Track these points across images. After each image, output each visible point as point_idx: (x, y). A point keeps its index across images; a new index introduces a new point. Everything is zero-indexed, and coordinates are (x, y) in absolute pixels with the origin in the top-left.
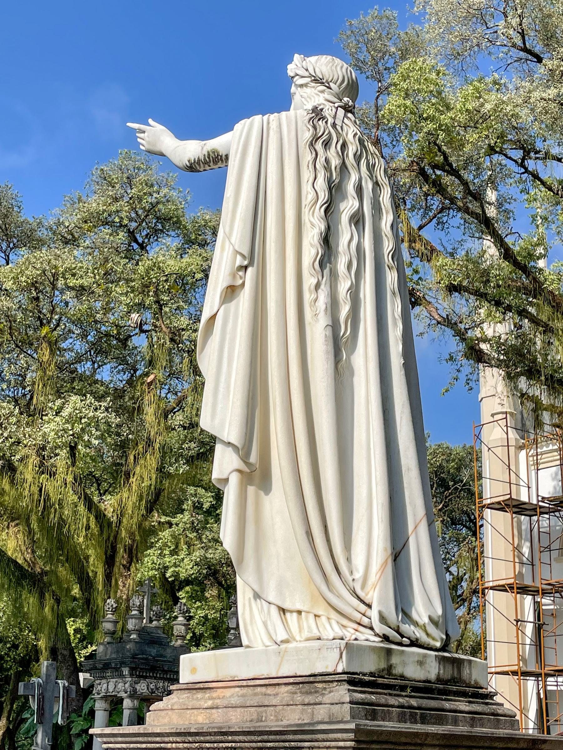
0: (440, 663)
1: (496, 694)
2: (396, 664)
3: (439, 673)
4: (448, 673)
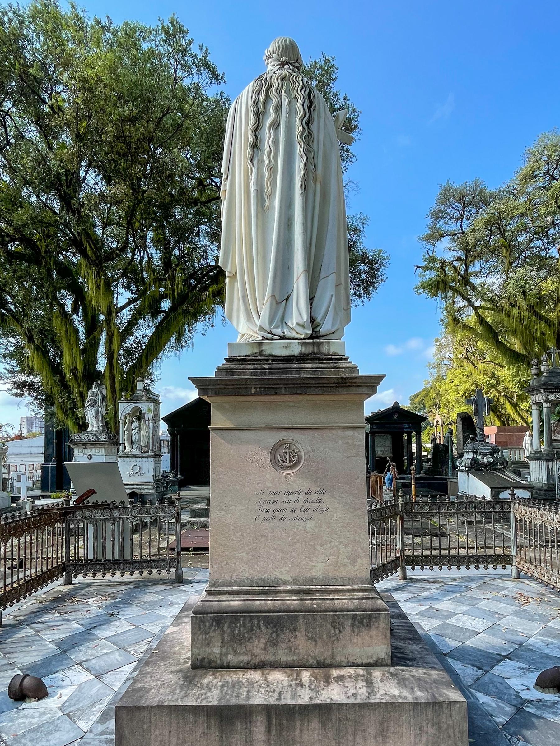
0: (302, 346)
4: (310, 349)
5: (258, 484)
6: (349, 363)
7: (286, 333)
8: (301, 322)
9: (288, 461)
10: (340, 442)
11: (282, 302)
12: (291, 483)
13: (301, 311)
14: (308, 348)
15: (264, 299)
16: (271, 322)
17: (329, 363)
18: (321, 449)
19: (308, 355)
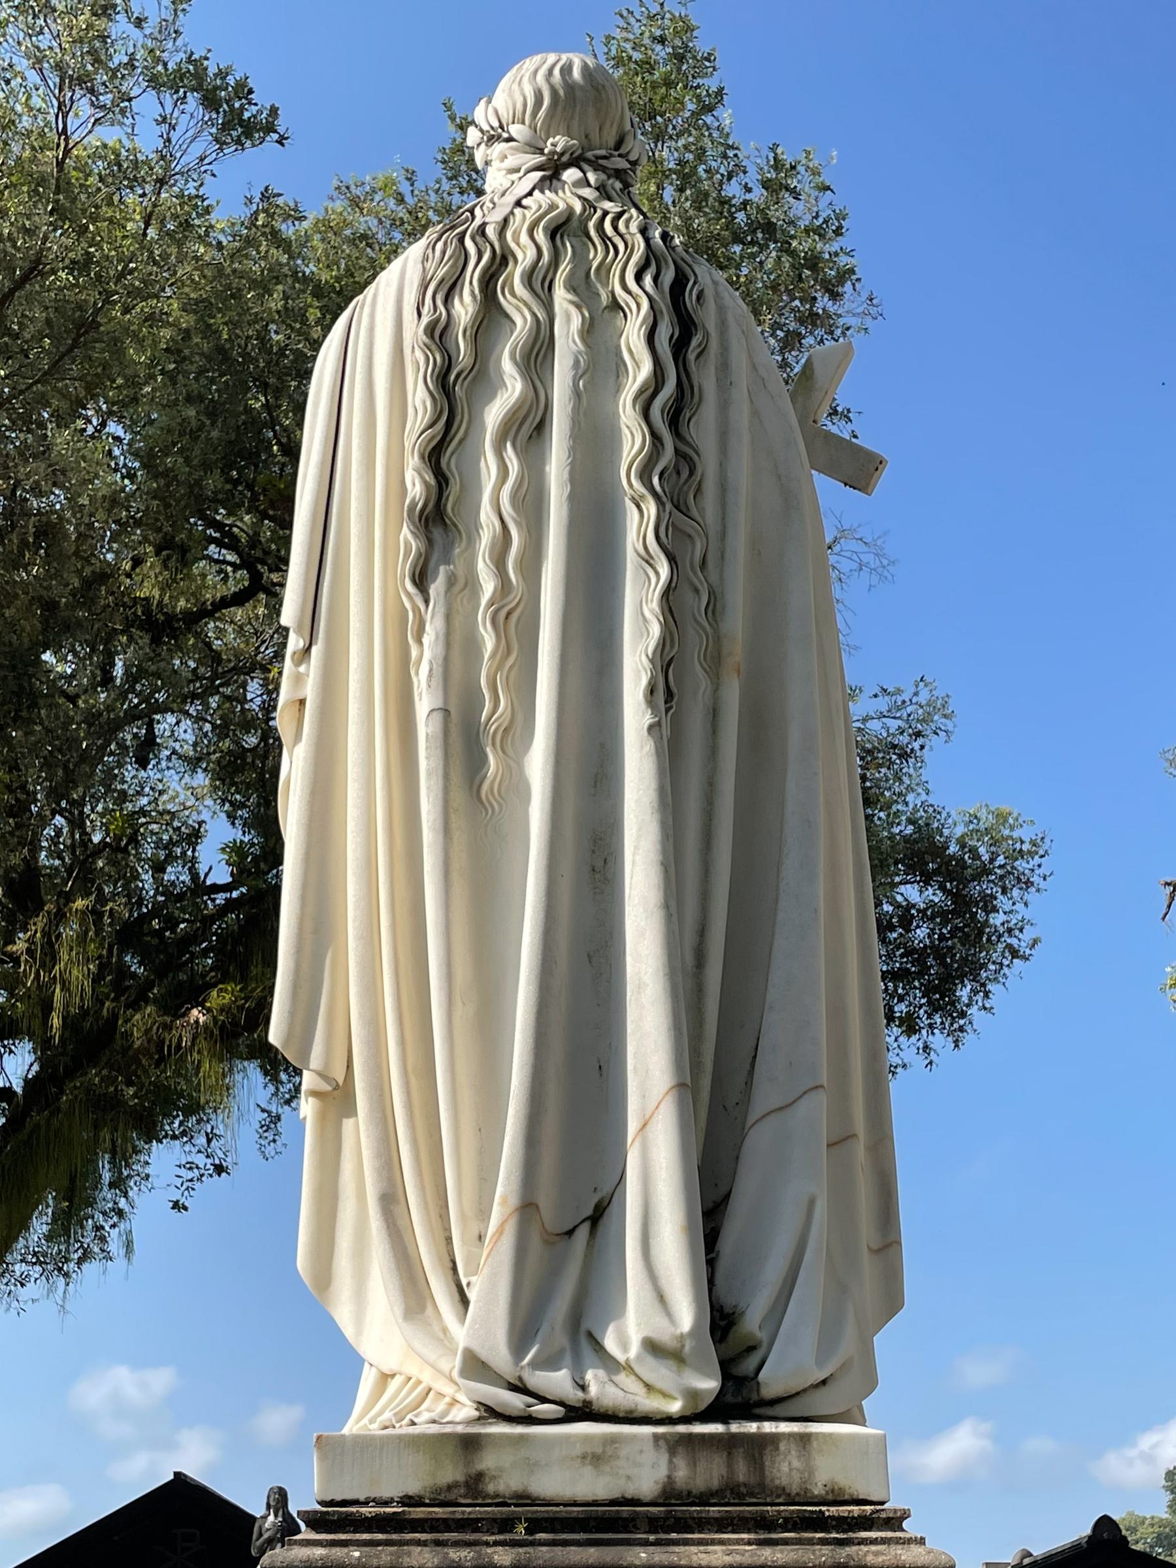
1: (905, 1515)
2: (501, 1469)
3: (669, 1477)
6: (909, 1541)
7: (593, 1390)
8: (664, 1333)
11: (570, 1233)
13: (664, 1283)
14: (702, 1465)
15: (484, 1213)
16: (521, 1338)
17: (811, 1542)
19: (703, 1499)
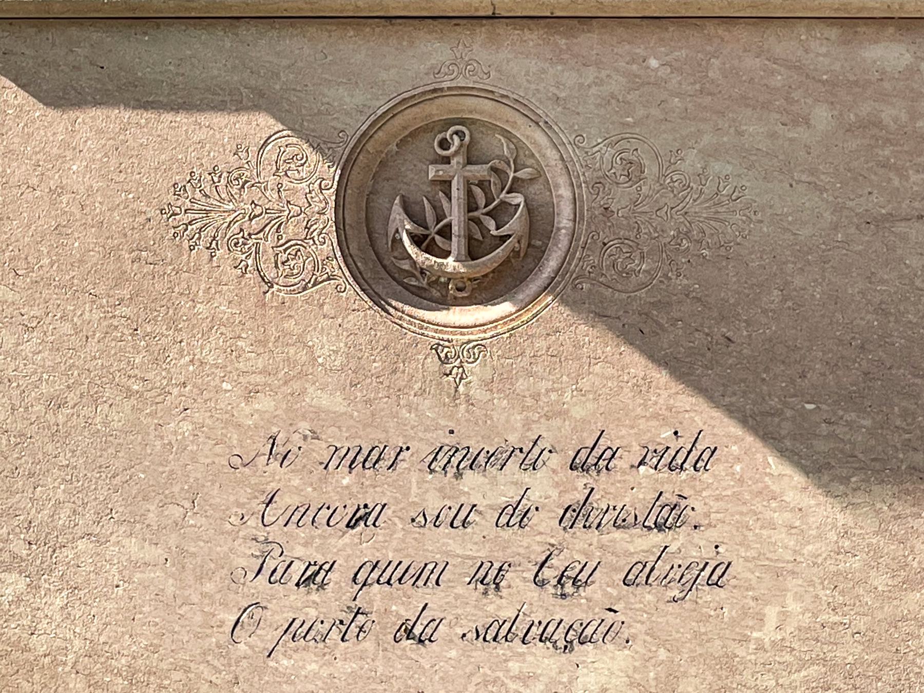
5: (251, 393)
9: (456, 244)
10: (822, 115)
12: (477, 393)
18: (691, 161)
